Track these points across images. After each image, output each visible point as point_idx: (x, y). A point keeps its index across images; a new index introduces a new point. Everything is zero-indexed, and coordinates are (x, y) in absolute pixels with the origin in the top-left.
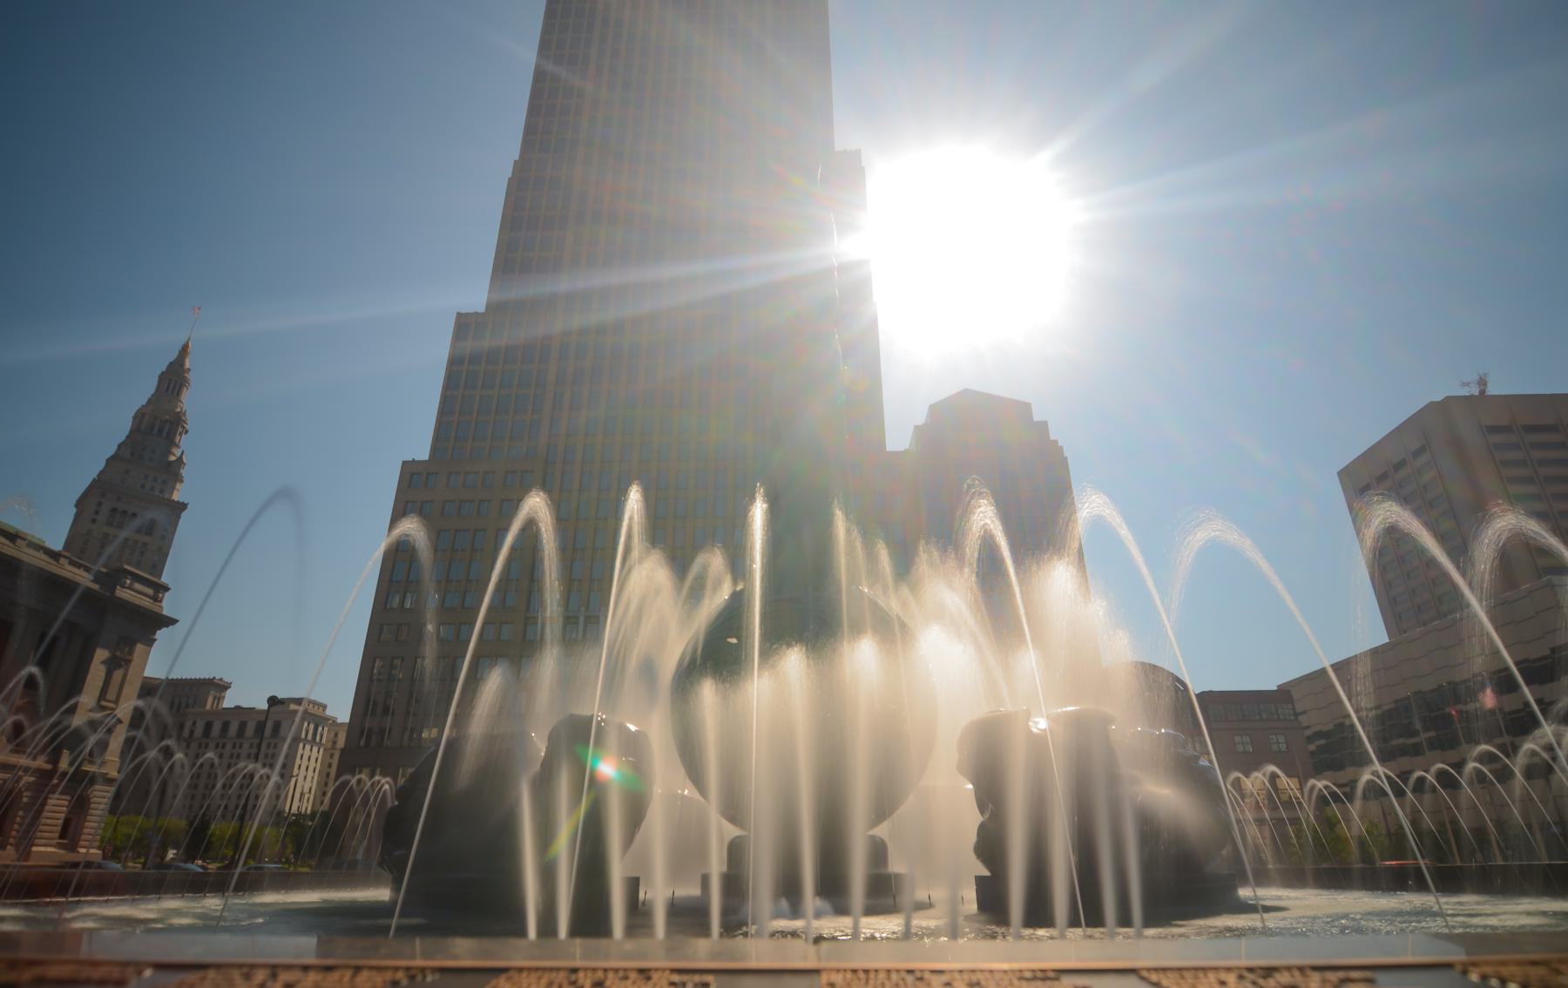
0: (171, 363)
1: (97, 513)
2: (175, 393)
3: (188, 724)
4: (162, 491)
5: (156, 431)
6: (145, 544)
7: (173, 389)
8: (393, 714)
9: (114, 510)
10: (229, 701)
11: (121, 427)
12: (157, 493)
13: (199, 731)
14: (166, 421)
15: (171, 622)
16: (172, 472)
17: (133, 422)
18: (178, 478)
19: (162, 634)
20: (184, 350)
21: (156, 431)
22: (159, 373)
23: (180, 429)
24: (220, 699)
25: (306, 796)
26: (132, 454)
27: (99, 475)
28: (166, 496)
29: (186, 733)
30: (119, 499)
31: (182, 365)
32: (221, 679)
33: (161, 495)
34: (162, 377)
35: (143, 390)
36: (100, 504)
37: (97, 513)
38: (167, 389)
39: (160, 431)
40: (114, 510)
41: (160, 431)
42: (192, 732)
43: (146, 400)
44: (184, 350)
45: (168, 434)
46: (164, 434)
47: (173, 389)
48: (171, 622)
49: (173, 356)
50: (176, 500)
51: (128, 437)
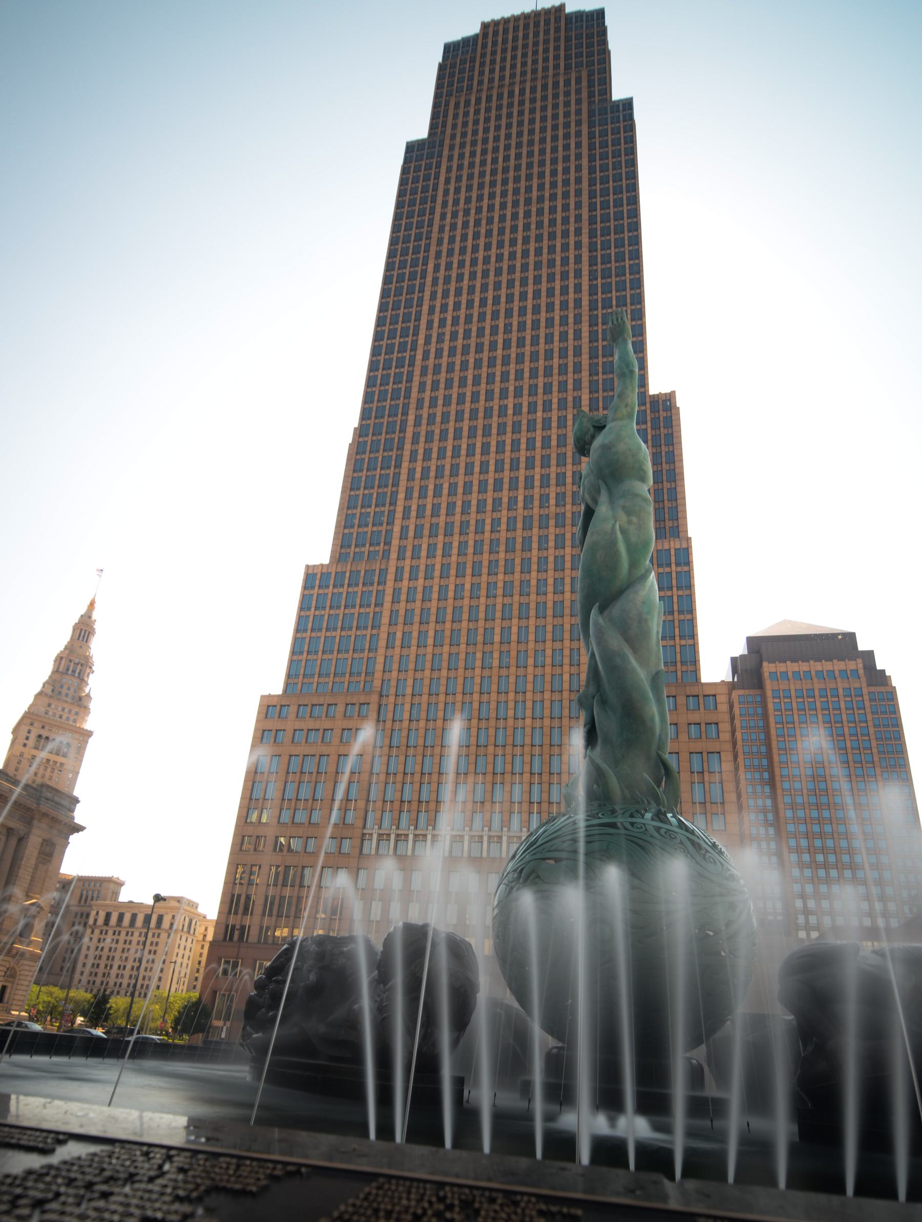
0: (82, 616)
1: (27, 738)
3: (93, 913)
4: (75, 721)
5: (70, 672)
7: (84, 637)
8: (251, 914)
9: (40, 736)
10: (124, 897)
11: (45, 671)
12: (71, 723)
13: (101, 921)
14: (77, 664)
15: (78, 829)
16: (81, 703)
17: (54, 665)
18: (86, 710)
19: (74, 838)
20: (92, 605)
21: (70, 672)
22: (73, 624)
24: (116, 894)
25: (183, 979)
26: (53, 691)
27: (29, 708)
28: (78, 725)
29: (91, 921)
30: (43, 727)
31: (90, 617)
32: (118, 878)
34: (75, 628)
35: (62, 638)
36: (29, 732)
37: (27, 738)
38: (78, 639)
39: (74, 671)
40: (40, 736)
41: (74, 671)
42: (96, 920)
43: (64, 647)
44: (92, 605)
45: (79, 674)
46: (77, 675)
47: (84, 637)
48: (78, 829)
49: (83, 610)
51: (50, 677)
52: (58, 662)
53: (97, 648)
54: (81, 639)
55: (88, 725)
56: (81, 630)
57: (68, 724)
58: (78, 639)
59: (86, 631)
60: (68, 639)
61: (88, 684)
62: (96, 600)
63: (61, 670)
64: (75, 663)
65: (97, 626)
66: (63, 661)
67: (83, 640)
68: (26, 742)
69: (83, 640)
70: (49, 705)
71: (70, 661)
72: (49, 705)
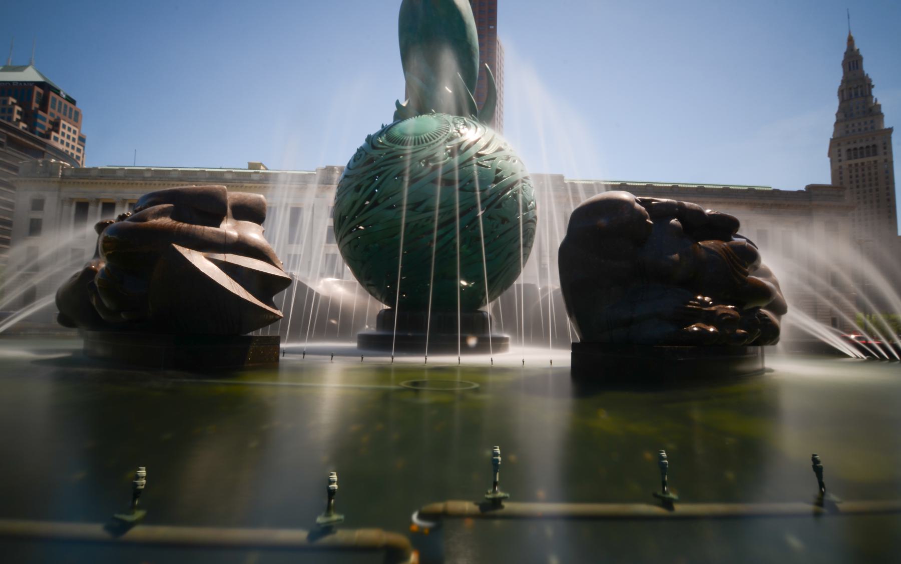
1: (840, 155)
5: (853, 96)
6: (875, 162)
7: (854, 67)
9: (849, 150)
14: (857, 88)
16: (875, 112)
20: (850, 40)
21: (853, 96)
26: (846, 116)
30: (849, 143)
34: (844, 64)
36: (839, 151)
37: (840, 155)
39: (856, 94)
41: (856, 94)
44: (850, 40)
45: (862, 93)
46: (859, 95)
47: (853, 64)
49: (844, 48)
53: (869, 68)
55: (887, 125)
61: (872, 97)
68: (840, 158)
70: (847, 126)
72: (847, 126)
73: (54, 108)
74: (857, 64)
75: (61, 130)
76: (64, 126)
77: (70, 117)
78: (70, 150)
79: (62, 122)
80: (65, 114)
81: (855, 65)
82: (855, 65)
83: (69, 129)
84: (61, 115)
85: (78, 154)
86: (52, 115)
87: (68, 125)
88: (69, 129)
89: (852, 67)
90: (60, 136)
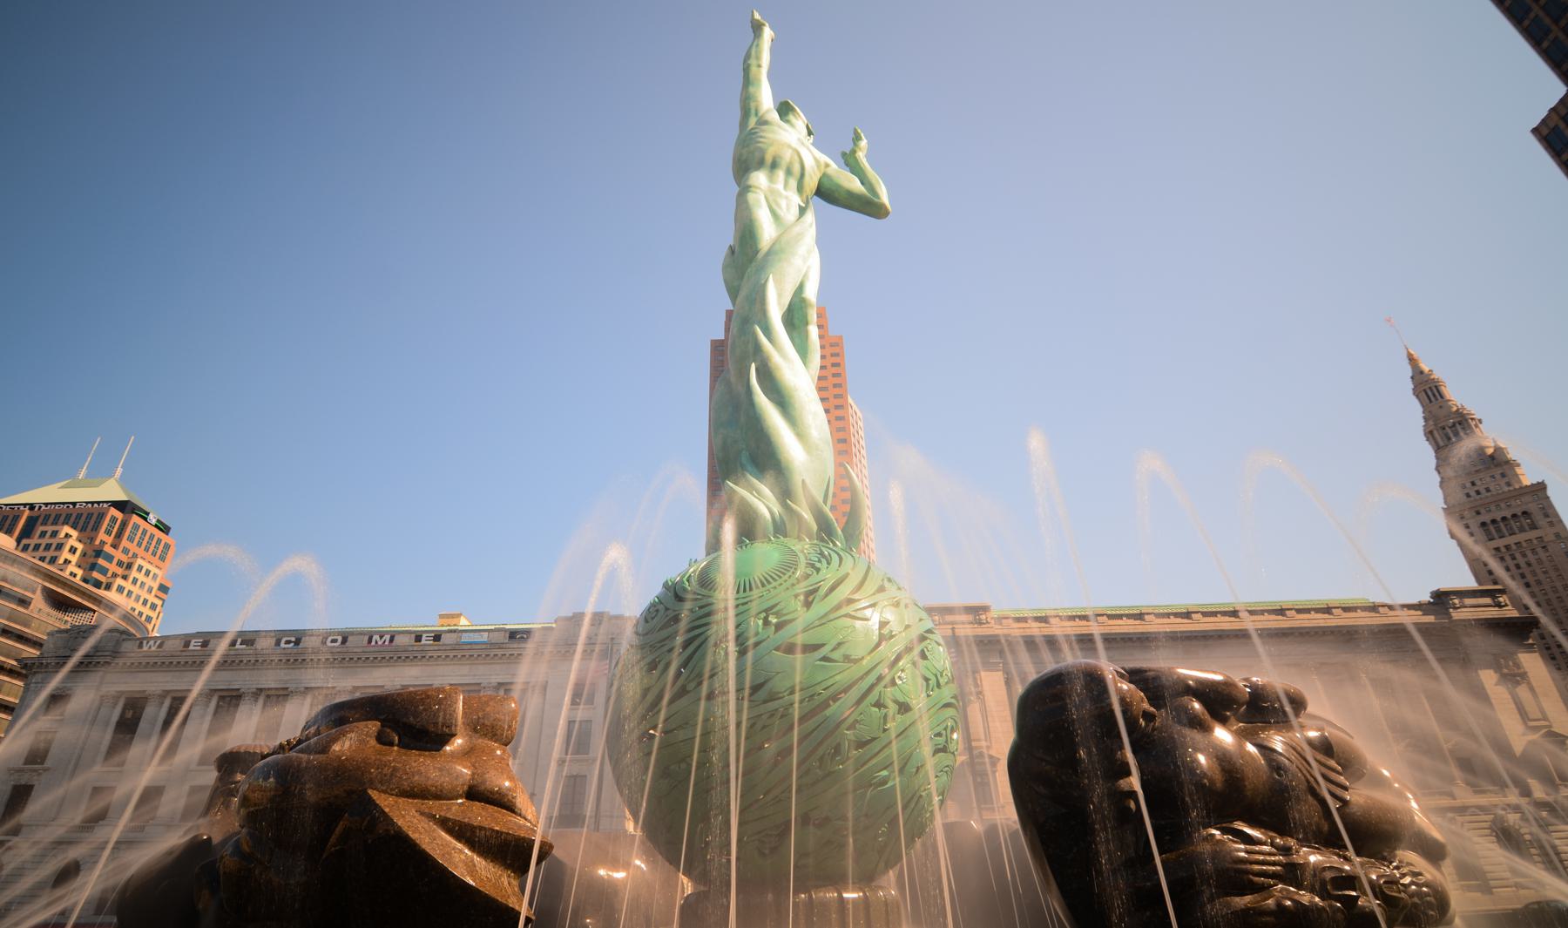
0: (1412, 378)
2: (1439, 397)
7: (1434, 395)
14: (1454, 425)
17: (1430, 444)
23: (1473, 423)
27: (1446, 503)
28: (1517, 486)
31: (1422, 372)
33: (1511, 488)
35: (1414, 412)
38: (1431, 401)
43: (1422, 421)
47: (1434, 395)
50: (1529, 484)
52: (1431, 438)
54: (1433, 399)
56: (1425, 390)
57: (1503, 492)
58: (1431, 401)
59: (1430, 388)
60: (1420, 409)
62: (1412, 352)
63: (1441, 444)
64: (1450, 427)
65: (1436, 375)
66: (1435, 432)
67: (1437, 399)
69: (1437, 399)
71: (1444, 429)
73: (131, 539)
74: (1438, 391)
75: (134, 573)
76: (140, 568)
77: (154, 554)
78: (139, 607)
79: (139, 561)
80: (147, 549)
81: (1437, 394)
82: (1437, 394)
83: (148, 573)
84: (140, 552)
85: (151, 613)
86: (126, 551)
87: (146, 566)
88: (148, 573)
89: (1433, 399)
90: (128, 585)
